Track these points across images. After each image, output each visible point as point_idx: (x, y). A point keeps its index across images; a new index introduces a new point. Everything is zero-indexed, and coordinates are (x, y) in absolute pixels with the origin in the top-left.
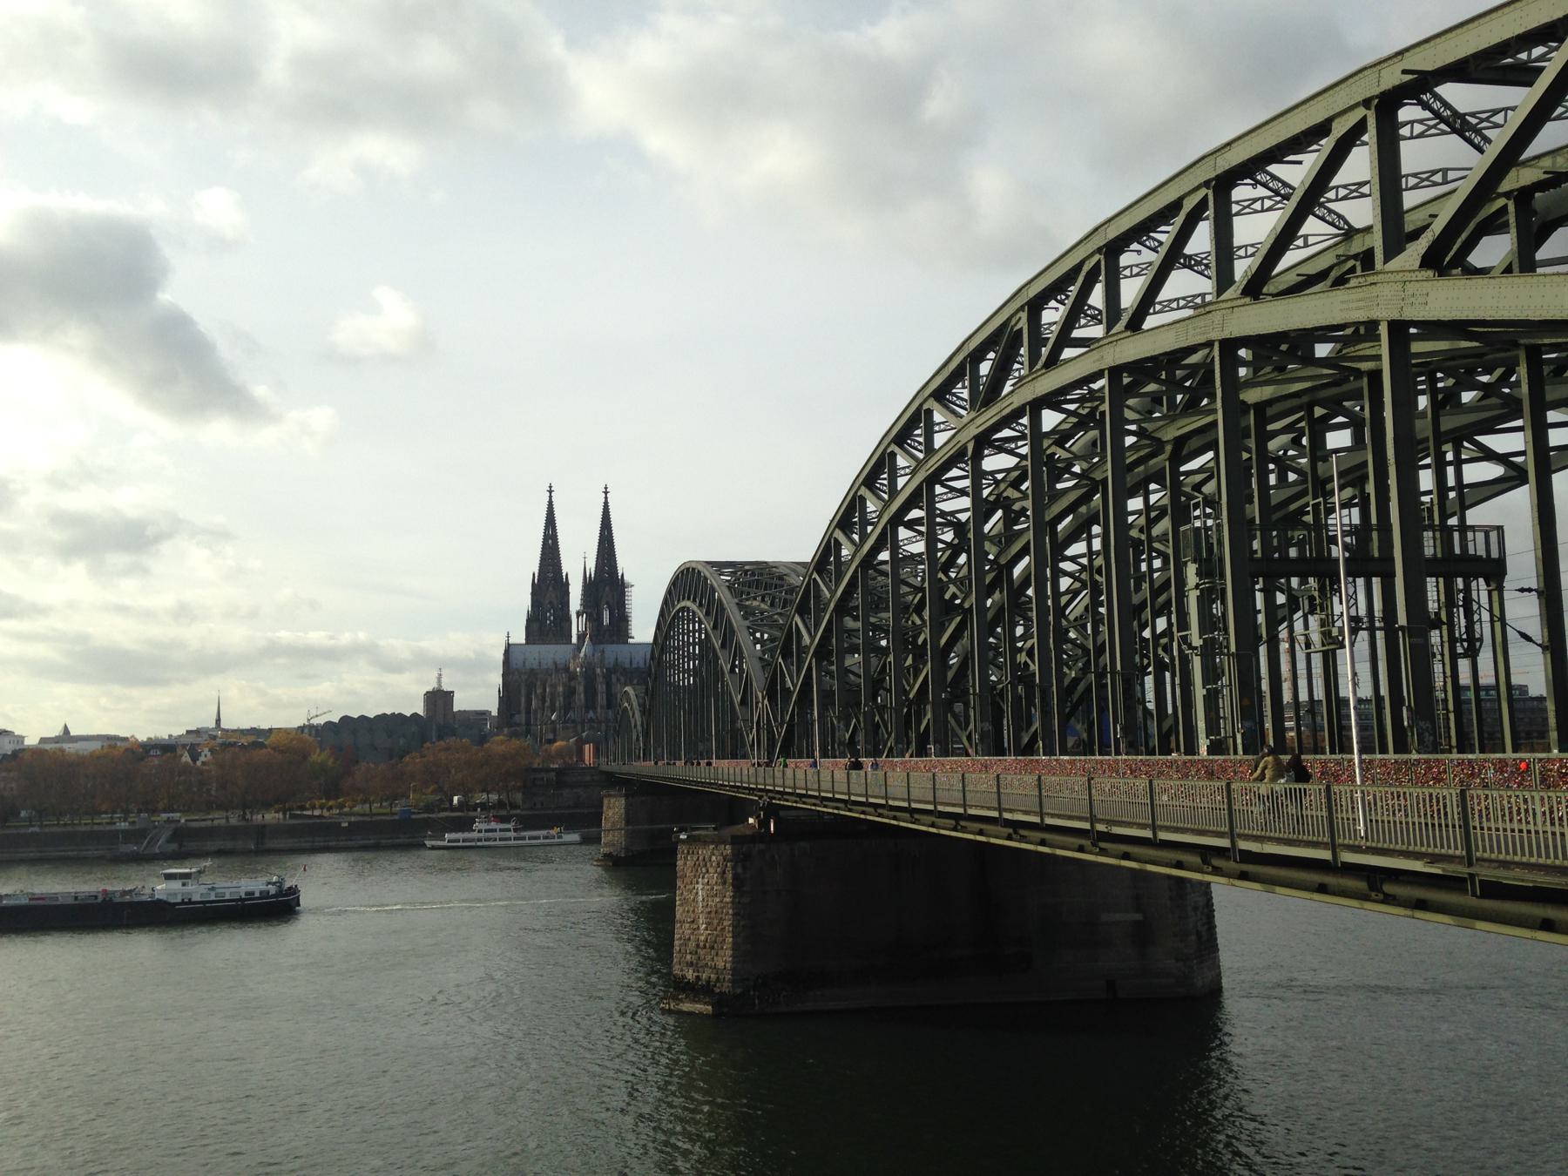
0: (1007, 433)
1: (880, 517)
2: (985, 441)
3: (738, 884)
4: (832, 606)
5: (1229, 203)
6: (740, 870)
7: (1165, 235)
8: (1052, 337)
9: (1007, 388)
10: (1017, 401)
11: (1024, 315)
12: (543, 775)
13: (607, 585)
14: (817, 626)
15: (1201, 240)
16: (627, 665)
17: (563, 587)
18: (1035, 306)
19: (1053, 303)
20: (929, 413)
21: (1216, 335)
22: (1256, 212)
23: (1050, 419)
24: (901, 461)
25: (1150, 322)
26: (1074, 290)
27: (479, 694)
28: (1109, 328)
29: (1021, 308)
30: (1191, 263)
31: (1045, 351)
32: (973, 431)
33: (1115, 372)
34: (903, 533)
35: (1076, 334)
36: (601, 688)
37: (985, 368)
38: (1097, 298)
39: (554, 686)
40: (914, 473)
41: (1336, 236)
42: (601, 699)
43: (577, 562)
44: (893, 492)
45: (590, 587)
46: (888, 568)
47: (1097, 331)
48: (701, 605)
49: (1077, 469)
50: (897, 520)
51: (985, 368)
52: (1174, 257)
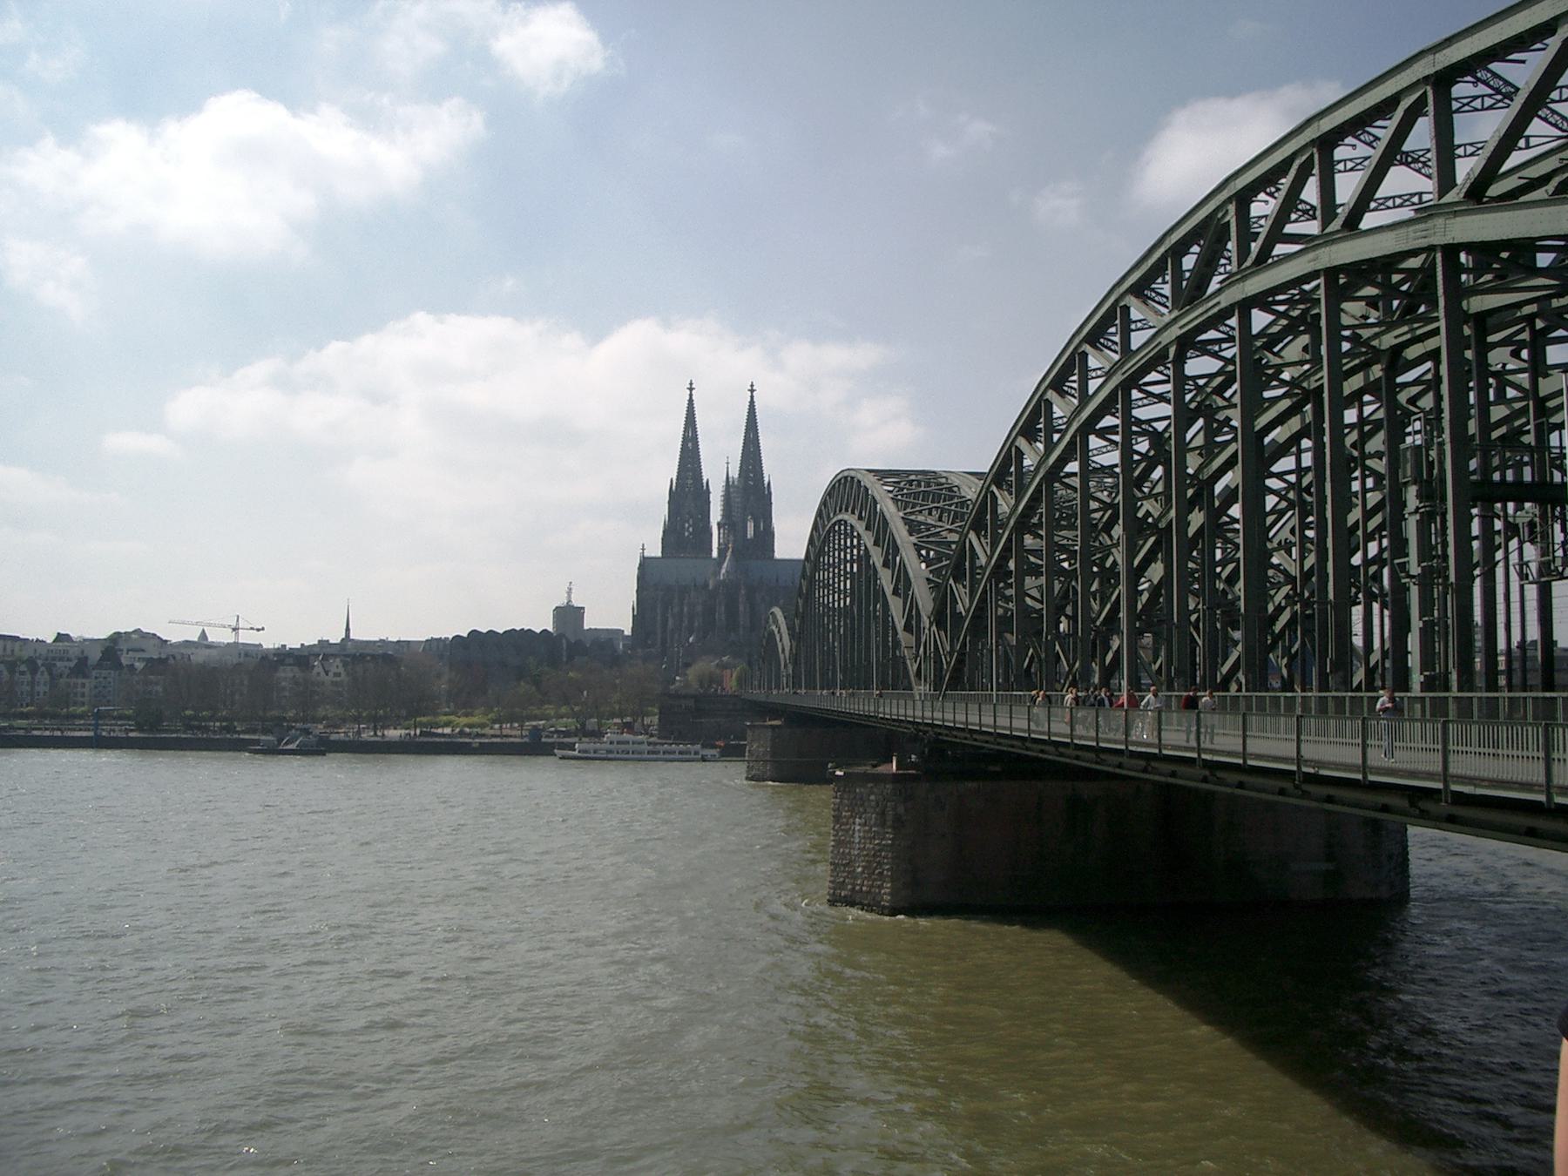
0: (1212, 334)
1: (1069, 423)
2: (1188, 344)
3: (898, 823)
4: (1012, 522)
5: (1449, 99)
6: (901, 809)
7: (1384, 130)
8: (1264, 232)
9: (1214, 286)
10: (1225, 300)
11: (1232, 208)
13: (751, 492)
14: (994, 545)
15: (1422, 135)
17: (703, 494)
18: (1244, 199)
19: (1262, 196)
21: (1438, 240)
22: (1476, 110)
23: (1260, 319)
24: (1093, 362)
25: (1369, 221)
26: (1285, 182)
27: (612, 609)
28: (1325, 225)
29: (1229, 200)
30: (1409, 160)
31: (1255, 247)
32: (1175, 332)
33: (1331, 273)
34: (1094, 442)
35: (1289, 229)
37: (1189, 262)
38: (1311, 193)
40: (1109, 375)
41: (1560, 138)
44: (1085, 398)
46: (1075, 481)
47: (1312, 228)
48: (860, 518)
49: (1286, 376)
50: (1089, 427)
51: (1189, 262)
52: (1393, 154)
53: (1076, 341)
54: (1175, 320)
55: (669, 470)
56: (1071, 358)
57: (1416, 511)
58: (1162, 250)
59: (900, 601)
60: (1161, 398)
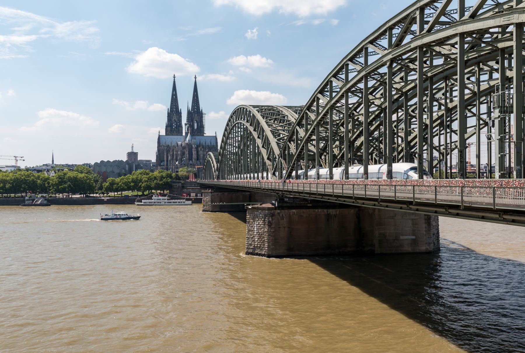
3: (270, 224)
4: (315, 123)
6: (270, 219)
11: (418, 13)
12: (177, 184)
16: (204, 144)
17: (179, 114)
21: (515, 21)
27: (148, 153)
29: (417, 9)
32: (390, 57)
34: (350, 94)
36: (194, 153)
37: (396, 31)
39: (177, 151)
40: (359, 72)
42: (194, 156)
43: (185, 105)
44: (347, 81)
45: (189, 113)
48: (247, 122)
51: (396, 31)
53: (345, 61)
54: (390, 53)
56: (343, 65)
57: (499, 116)
58: (385, 28)
59: (265, 151)
60: (374, 79)
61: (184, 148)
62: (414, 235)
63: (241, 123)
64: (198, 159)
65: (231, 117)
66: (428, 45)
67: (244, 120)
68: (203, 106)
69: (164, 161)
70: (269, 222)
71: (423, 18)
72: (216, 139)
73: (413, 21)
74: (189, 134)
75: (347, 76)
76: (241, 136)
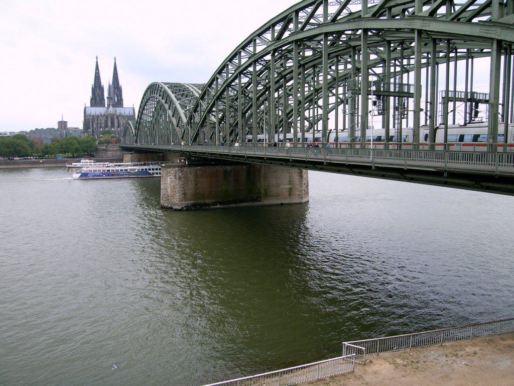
1: (235, 71)
3: (180, 178)
6: (180, 175)
11: (294, 14)
13: (116, 87)
17: (102, 89)
20: (255, 40)
24: (243, 54)
27: (76, 122)
32: (273, 47)
34: (242, 75)
37: (278, 28)
39: (101, 120)
42: (116, 124)
43: (106, 81)
48: (160, 95)
51: (278, 28)
55: (92, 82)
60: (261, 64)
61: (107, 117)
62: (290, 184)
63: (154, 97)
64: (118, 127)
65: (146, 91)
66: (301, 40)
67: (157, 94)
68: (122, 82)
69: (90, 128)
70: (179, 177)
71: (298, 19)
72: (134, 110)
73: (290, 21)
74: (111, 107)
75: (240, 61)
76: (155, 108)
